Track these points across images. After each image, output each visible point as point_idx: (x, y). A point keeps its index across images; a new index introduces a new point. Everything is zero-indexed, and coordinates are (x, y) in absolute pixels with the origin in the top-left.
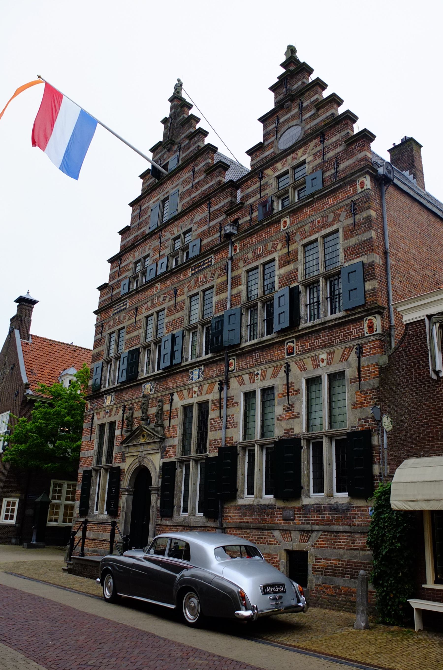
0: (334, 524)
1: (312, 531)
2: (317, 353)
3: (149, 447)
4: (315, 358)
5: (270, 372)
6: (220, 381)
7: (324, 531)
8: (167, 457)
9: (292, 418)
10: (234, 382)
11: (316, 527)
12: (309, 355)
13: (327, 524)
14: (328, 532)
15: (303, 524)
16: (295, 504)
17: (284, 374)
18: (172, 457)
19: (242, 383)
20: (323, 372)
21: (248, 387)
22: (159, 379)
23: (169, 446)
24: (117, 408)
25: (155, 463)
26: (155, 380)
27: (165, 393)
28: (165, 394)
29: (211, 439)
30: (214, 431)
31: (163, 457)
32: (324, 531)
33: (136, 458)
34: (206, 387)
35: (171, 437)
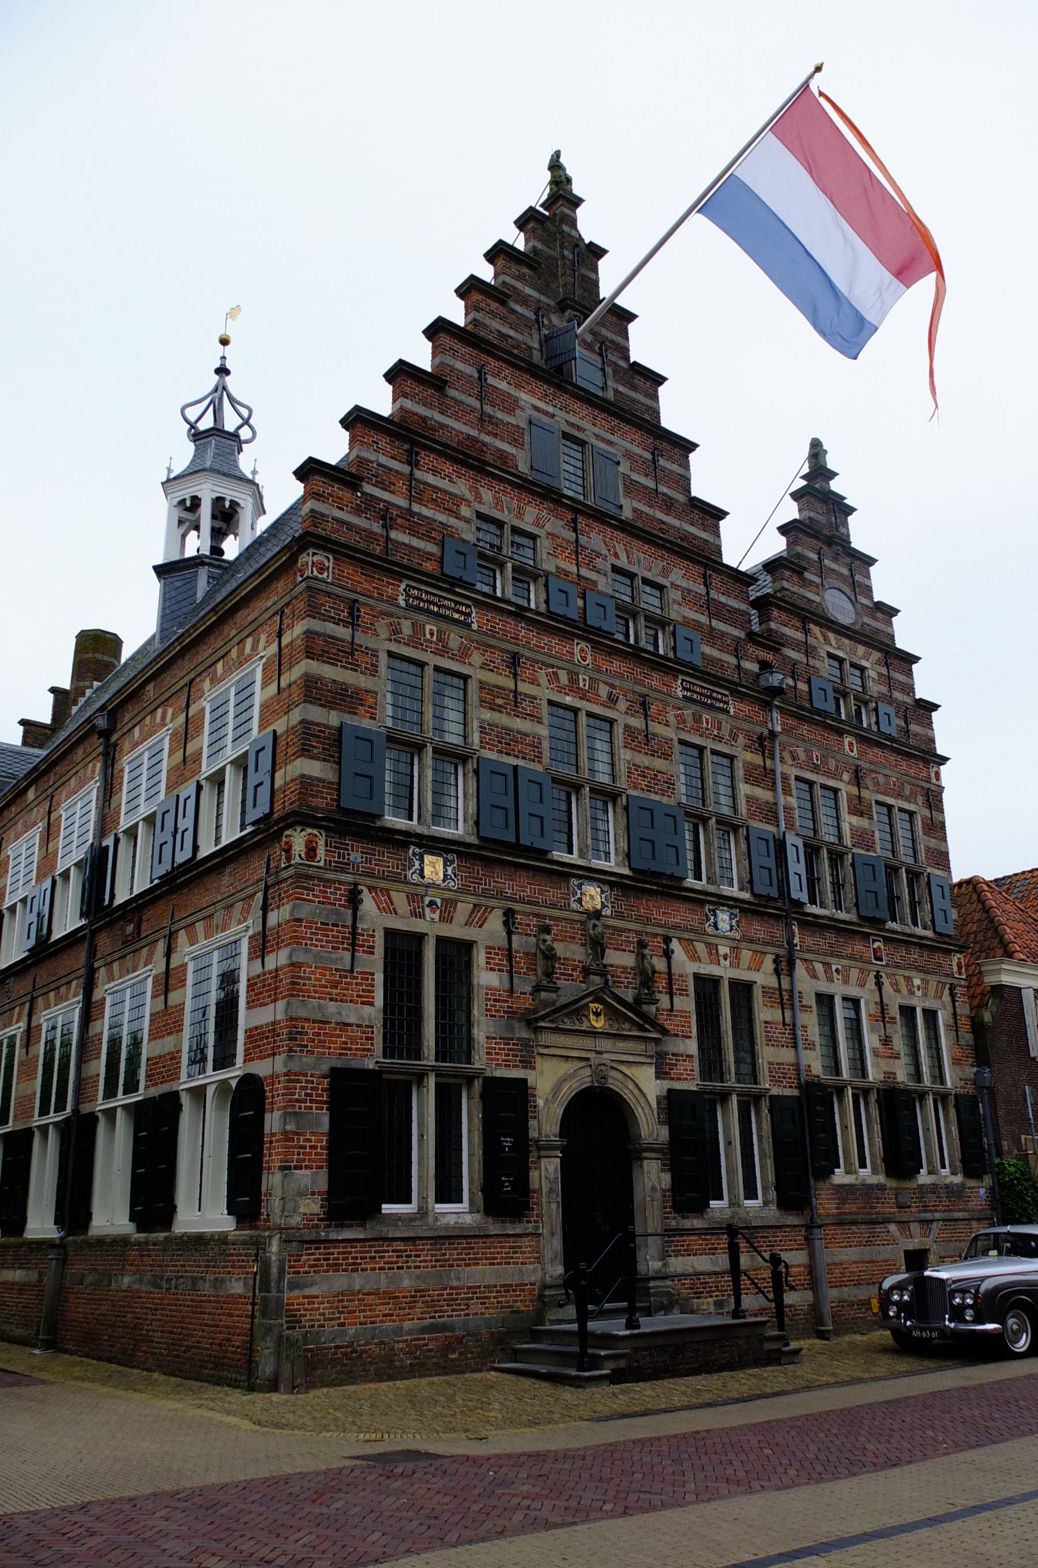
0: (951, 1211)
1: (932, 1221)
2: (913, 974)
4: (908, 979)
5: (854, 974)
6: (777, 956)
7: (944, 1220)
8: (672, 1079)
9: (891, 1057)
10: (800, 970)
11: (938, 1215)
12: (901, 972)
13: (945, 1211)
14: (947, 1220)
15: (920, 1212)
17: (874, 987)
18: (685, 1079)
19: (814, 976)
20: (919, 1004)
21: (825, 987)
22: (624, 887)
23: (673, 1055)
24: (475, 906)
25: (645, 1087)
26: (612, 885)
27: (649, 929)
28: (648, 930)
29: (771, 1060)
30: (773, 1045)
31: (660, 1075)
32: (944, 1220)
33: (582, 1064)
34: (746, 955)
35: (677, 1035)
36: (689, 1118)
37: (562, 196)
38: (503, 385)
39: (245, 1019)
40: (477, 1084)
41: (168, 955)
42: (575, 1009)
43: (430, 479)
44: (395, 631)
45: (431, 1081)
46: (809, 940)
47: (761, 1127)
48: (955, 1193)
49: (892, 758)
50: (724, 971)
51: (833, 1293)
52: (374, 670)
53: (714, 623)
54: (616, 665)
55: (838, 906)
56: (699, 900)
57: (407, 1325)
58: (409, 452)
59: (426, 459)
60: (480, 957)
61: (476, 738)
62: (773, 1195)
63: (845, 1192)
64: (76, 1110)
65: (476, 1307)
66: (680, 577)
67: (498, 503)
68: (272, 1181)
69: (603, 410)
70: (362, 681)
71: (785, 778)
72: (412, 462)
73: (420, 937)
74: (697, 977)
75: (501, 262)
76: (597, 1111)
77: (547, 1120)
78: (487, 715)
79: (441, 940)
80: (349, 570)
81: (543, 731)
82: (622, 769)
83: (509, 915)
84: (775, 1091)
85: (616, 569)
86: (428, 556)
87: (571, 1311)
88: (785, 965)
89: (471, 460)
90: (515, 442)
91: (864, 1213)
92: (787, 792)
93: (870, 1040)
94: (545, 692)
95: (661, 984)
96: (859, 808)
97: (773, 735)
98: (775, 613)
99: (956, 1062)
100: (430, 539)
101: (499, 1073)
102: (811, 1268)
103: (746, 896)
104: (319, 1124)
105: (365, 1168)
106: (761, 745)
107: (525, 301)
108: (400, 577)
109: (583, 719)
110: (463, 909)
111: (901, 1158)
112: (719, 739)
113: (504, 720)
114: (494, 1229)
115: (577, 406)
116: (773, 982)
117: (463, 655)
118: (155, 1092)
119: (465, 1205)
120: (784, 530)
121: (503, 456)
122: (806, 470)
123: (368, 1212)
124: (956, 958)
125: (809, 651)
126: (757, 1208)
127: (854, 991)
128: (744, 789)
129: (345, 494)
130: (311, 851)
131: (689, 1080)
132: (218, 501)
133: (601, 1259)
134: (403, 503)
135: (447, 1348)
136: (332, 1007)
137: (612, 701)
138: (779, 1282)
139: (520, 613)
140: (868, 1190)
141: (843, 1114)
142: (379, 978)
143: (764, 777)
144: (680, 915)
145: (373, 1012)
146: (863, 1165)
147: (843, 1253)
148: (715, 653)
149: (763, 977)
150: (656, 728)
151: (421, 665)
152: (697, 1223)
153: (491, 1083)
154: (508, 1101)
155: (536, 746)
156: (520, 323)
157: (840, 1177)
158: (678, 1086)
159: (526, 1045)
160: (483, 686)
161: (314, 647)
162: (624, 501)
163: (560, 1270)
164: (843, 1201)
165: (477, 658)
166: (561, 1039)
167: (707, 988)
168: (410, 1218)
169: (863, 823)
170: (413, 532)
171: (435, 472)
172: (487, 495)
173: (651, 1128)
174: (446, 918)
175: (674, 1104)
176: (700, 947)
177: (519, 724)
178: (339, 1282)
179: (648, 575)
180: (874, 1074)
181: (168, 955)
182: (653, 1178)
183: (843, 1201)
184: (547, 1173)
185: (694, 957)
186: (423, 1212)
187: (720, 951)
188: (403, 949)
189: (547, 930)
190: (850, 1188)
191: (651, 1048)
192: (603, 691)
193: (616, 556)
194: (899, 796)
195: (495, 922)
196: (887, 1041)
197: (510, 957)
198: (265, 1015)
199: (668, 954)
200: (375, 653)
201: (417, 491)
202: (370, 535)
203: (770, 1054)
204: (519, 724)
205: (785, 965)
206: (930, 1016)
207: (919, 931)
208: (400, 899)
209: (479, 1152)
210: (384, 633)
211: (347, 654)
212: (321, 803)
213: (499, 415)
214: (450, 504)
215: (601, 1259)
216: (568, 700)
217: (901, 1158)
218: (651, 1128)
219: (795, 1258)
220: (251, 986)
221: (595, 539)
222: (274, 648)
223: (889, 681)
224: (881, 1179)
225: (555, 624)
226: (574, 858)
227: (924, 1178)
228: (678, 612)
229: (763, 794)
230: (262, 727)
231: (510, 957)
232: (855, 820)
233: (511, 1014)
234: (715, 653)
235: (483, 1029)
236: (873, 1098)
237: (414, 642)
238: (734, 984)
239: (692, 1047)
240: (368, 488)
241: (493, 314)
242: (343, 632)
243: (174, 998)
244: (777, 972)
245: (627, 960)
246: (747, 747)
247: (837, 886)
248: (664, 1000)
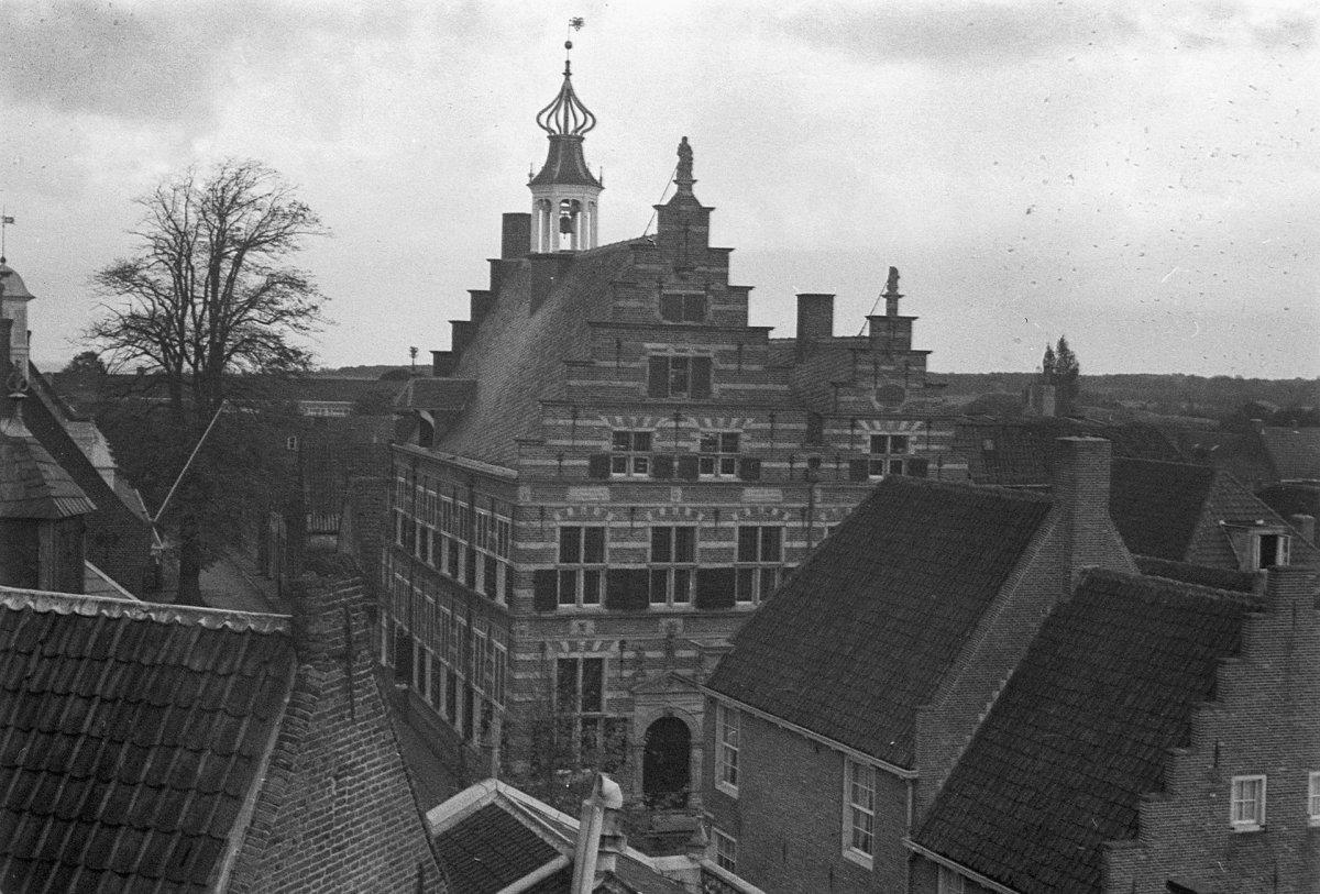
67: (627, 423)
77: (638, 735)
106: (803, 515)
110: (597, 646)
122: (886, 291)
165: (611, 516)
171: (588, 417)
172: (619, 419)
174: (589, 648)
192: (688, 512)
193: (705, 426)
195: (615, 646)
200: (553, 530)
211: (540, 535)
214: (599, 434)
228: (747, 446)
240: (551, 442)
242: (537, 524)
246: (791, 519)
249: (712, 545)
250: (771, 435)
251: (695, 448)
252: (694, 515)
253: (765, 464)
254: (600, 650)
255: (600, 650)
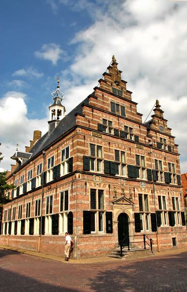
3: (129, 206)
10: (155, 192)
16: (173, 227)
20: (175, 197)
21: (159, 195)
25: (131, 213)
31: (133, 210)
34: (147, 190)
36: (137, 216)
37: (114, 63)
38: (106, 97)
39: (70, 203)
40: (105, 213)
41: (56, 191)
42: (119, 200)
43: (95, 114)
44: (91, 140)
45: (98, 212)
46: (157, 187)
47: (149, 217)
48: (181, 228)
49: (171, 155)
50: (143, 193)
51: (161, 245)
52: (88, 147)
53: (141, 134)
54: (126, 143)
55: (162, 181)
56: (139, 181)
57: (95, 250)
58: (93, 110)
59: (95, 110)
60: (105, 192)
61: (103, 157)
62: (151, 229)
63: (163, 228)
64: (42, 216)
65: (105, 247)
66: (135, 127)
68: (74, 228)
69: (122, 99)
70: (86, 148)
71: (153, 160)
72: (93, 112)
73: (96, 190)
74: (139, 194)
75: (106, 76)
76: (123, 217)
77: (115, 218)
78: (105, 153)
79: (99, 190)
80: (83, 130)
81: (114, 155)
82: (126, 160)
83: (109, 185)
84: (151, 212)
85: (125, 126)
86: (95, 127)
87: (120, 248)
88: (153, 192)
89: (102, 110)
90: (108, 106)
91: (165, 232)
92: (153, 162)
93: (167, 203)
94: (114, 148)
95: (133, 196)
96: (165, 164)
97: (151, 153)
98: (151, 131)
99: (181, 206)
100: (95, 124)
101: (108, 211)
102: (157, 241)
103: (147, 180)
104: (81, 219)
105: (88, 227)
107: (109, 82)
108: (91, 131)
109: (120, 152)
110: (102, 185)
111: (172, 223)
112: (142, 154)
113: (107, 153)
114: (108, 235)
115: (118, 99)
116: (151, 194)
117: (101, 143)
118: (55, 213)
119: (103, 232)
120: (152, 116)
121: (107, 109)
123: (89, 233)
124: (181, 189)
125: (157, 137)
126: (149, 231)
127: (164, 195)
128: (146, 162)
129: (83, 118)
130: (79, 177)
131: (138, 211)
132: (58, 110)
133: (124, 239)
134: (91, 118)
135: (101, 254)
136: (83, 201)
137: (125, 149)
138: (151, 244)
139: (110, 136)
140: (166, 228)
141: (162, 215)
142: (90, 196)
143: (149, 160)
144: (136, 184)
145: (89, 202)
146: (166, 224)
147: (161, 238)
148: (141, 139)
149: (149, 194)
150: (132, 153)
151: (95, 145)
152: (138, 234)
153: (106, 212)
154: (109, 216)
155: (113, 157)
156: (109, 86)
157: (162, 226)
158: (136, 212)
159: (112, 206)
160: (104, 148)
161: (78, 144)
162: (126, 114)
163: (118, 241)
164: (162, 230)
165: (103, 143)
166: (118, 205)
167: (140, 196)
168: (95, 234)
169: (166, 166)
170: (93, 123)
171: (96, 113)
172: (104, 116)
173: (132, 219)
174: (100, 187)
175: (135, 214)
176: (139, 189)
177: (110, 154)
178: (85, 243)
179: (130, 127)
180: (167, 209)
181: (56, 191)
182: (132, 227)
183: (162, 230)
184: (115, 227)
185: (139, 191)
186: (97, 233)
187: (143, 189)
188: (93, 192)
189: (115, 188)
190: (163, 228)
191: (131, 206)
192: (123, 147)
194: (172, 161)
196: (170, 203)
197: (109, 192)
198: (74, 202)
199: (134, 191)
201: (93, 116)
202: (87, 124)
203: (150, 206)
204: (110, 154)
205: (153, 192)
206: (177, 198)
207: (175, 184)
208: (93, 184)
209: (105, 223)
210: (89, 140)
211: (83, 144)
212: (80, 169)
213: (106, 102)
214: (98, 118)
215: (124, 239)
216: (118, 149)
217: (172, 223)
218: (132, 219)
219: (154, 239)
220: (70, 198)
221: (122, 121)
222: (72, 143)
223: (170, 142)
224: (169, 226)
225: (116, 136)
226: (119, 176)
227: (176, 226)
228: (135, 132)
229: (150, 163)
230: (71, 156)
231: (109, 192)
232: (165, 166)
233: (110, 201)
234: (141, 139)
235: (105, 204)
236: (167, 213)
237: (94, 141)
238: (145, 195)
239: (138, 206)
241: (104, 85)
242: (83, 141)
243: (57, 199)
244: (152, 193)
245: (128, 192)
247: (162, 178)
248: (134, 198)
249: (130, 158)
250: (140, 131)
251: (123, 129)
252: (125, 149)
253: (140, 139)
254: (103, 187)
255: (103, 187)
